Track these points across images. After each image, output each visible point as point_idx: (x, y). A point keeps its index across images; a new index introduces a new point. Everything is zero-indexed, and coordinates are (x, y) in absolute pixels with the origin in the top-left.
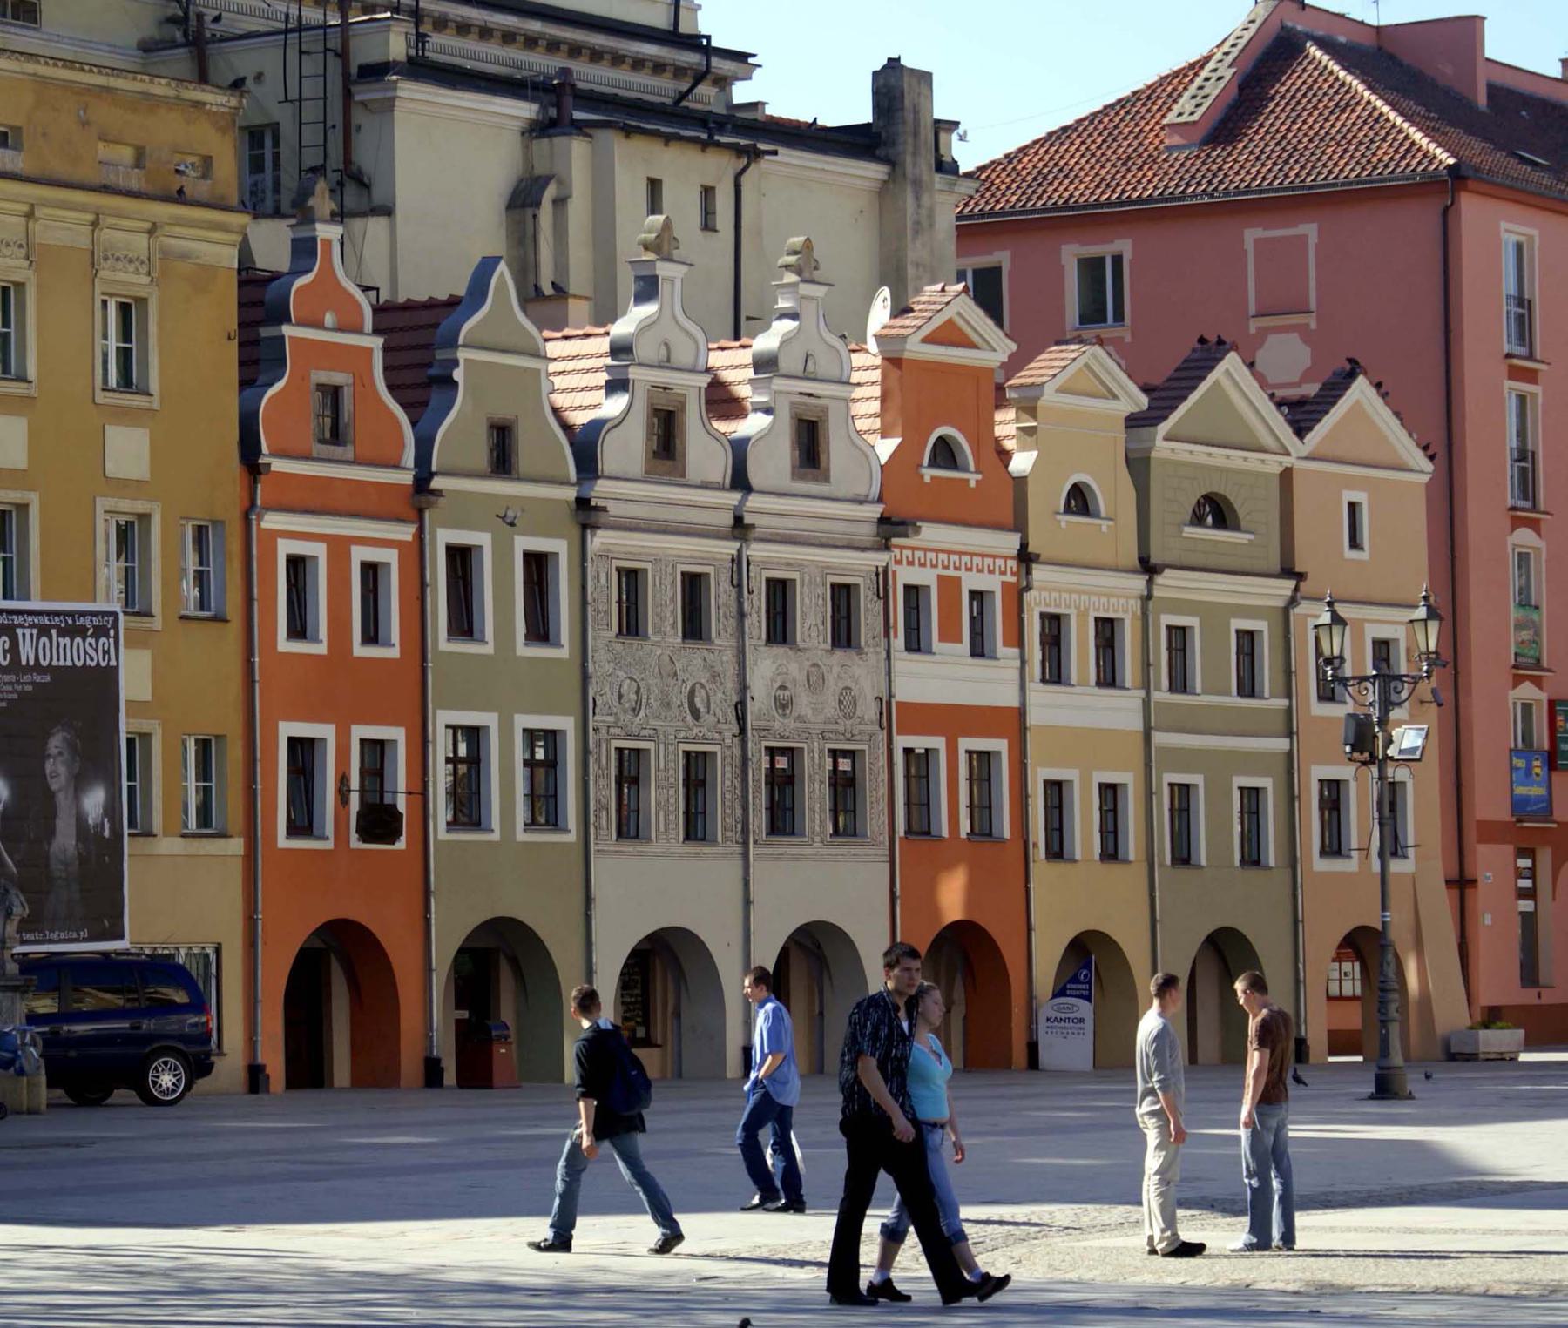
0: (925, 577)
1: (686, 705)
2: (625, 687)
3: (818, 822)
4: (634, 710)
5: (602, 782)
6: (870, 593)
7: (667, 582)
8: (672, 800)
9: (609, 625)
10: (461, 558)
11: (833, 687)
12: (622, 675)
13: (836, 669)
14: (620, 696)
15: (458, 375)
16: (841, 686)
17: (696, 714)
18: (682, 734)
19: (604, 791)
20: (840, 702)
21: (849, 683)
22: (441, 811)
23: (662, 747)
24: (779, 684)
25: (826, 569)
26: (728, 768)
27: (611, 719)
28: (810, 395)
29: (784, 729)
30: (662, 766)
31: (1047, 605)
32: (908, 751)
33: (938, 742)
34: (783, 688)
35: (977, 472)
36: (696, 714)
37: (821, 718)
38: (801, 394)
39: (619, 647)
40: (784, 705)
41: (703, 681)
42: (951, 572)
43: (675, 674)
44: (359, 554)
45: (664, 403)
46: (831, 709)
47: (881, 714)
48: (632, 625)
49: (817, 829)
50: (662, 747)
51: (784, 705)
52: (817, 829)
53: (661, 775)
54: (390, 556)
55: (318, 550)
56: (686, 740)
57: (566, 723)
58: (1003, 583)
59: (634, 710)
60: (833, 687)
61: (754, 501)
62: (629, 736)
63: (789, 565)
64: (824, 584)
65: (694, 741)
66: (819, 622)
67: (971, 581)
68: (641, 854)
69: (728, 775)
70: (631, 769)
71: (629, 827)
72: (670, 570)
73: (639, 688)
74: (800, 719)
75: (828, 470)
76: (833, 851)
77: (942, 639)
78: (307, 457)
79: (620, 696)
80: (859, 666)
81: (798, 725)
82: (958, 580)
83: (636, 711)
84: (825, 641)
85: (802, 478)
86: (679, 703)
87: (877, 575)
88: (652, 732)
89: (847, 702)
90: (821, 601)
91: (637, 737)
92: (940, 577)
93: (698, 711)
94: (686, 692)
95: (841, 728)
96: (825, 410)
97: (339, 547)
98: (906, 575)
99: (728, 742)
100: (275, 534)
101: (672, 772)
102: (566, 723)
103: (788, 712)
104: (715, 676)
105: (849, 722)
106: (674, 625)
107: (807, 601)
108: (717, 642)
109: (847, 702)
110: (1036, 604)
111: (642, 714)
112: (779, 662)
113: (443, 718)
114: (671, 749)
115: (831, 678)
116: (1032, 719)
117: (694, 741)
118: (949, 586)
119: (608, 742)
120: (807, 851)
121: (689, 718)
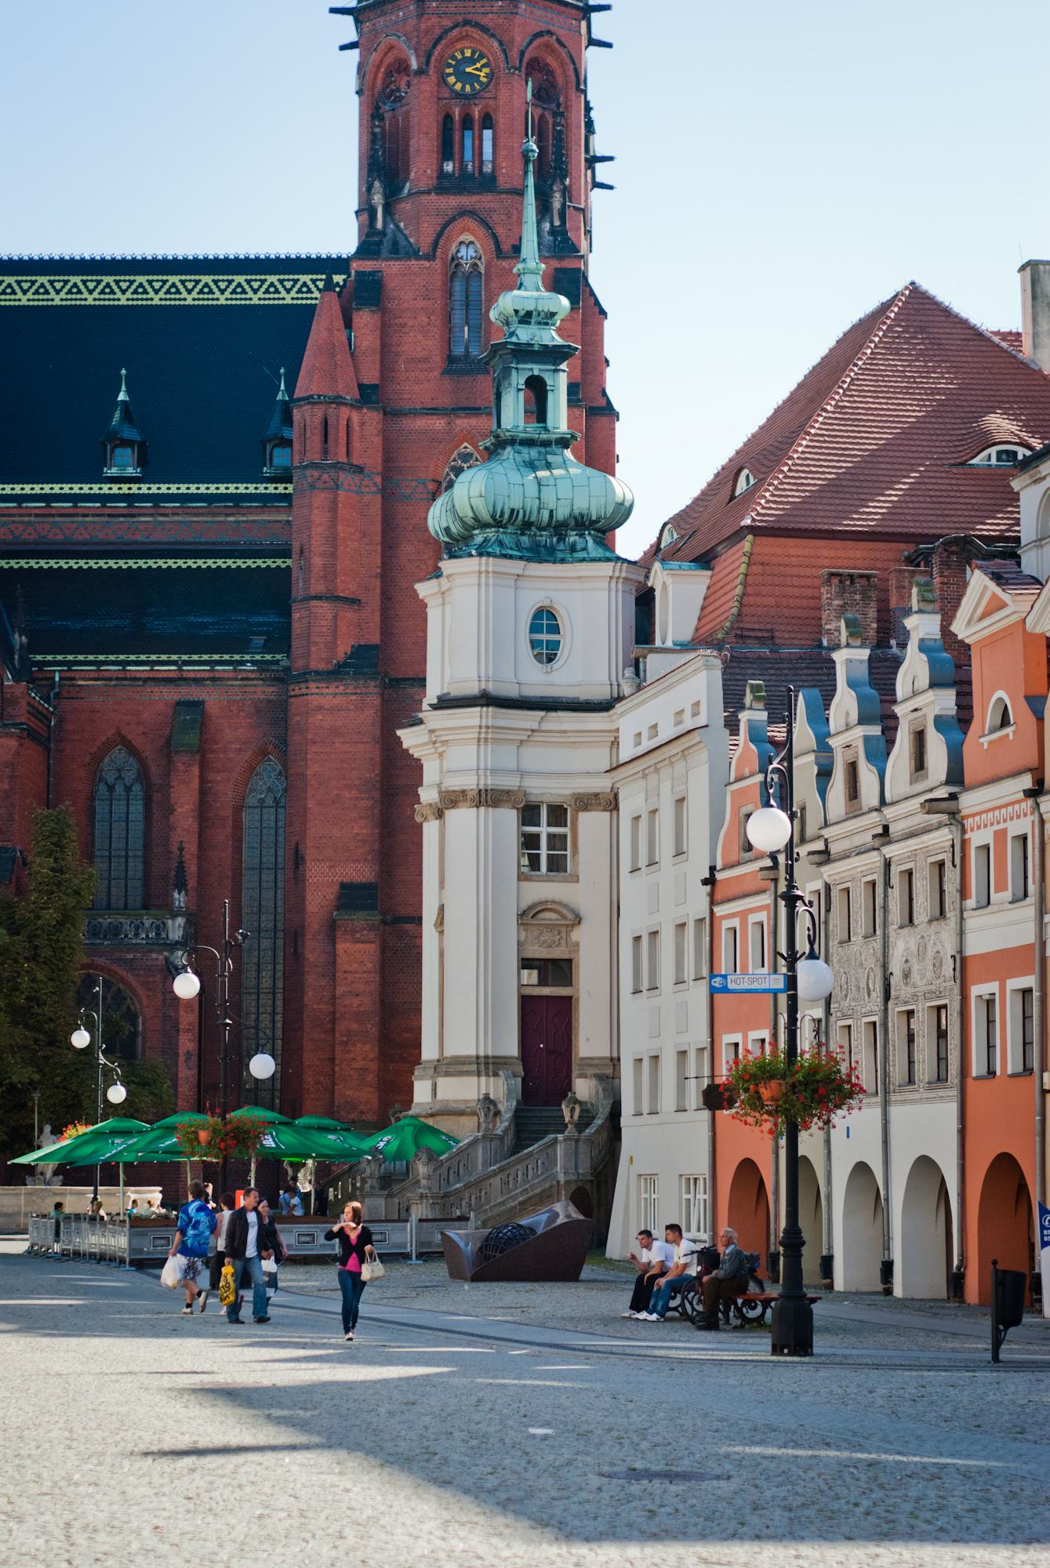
11: (930, 953)
25: (927, 851)
33: (993, 987)
34: (907, 961)
40: (907, 975)
42: (1002, 826)
44: (753, 918)
46: (930, 975)
47: (954, 969)
51: (907, 975)
55: (735, 922)
60: (930, 953)
61: (889, 812)
67: (1016, 828)
78: (738, 864)
82: (1005, 830)
85: (916, 782)
89: (938, 964)
95: (933, 988)
97: (743, 915)
120: (917, 1096)
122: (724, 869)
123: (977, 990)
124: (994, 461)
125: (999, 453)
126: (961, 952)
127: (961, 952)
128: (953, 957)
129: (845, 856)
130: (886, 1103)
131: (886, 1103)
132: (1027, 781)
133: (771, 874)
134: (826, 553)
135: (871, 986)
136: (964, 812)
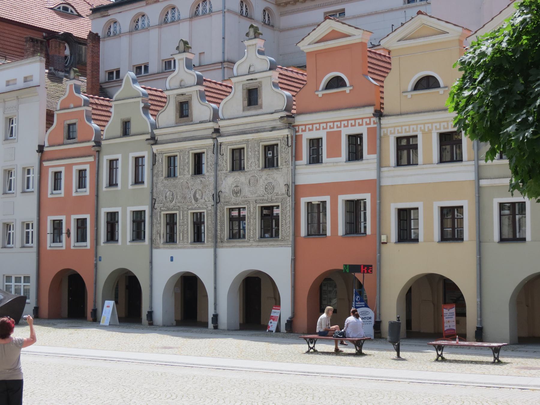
0: (321, 134)
1: (192, 197)
2: (168, 194)
3: (252, 233)
4: (171, 201)
5: (158, 225)
6: (284, 146)
7: (186, 157)
8: (186, 229)
9: (162, 175)
10: (112, 163)
12: (168, 190)
13: (263, 178)
14: (166, 197)
15: (112, 110)
16: (266, 182)
17: (196, 200)
18: (190, 207)
19: (162, 228)
20: (265, 188)
21: (271, 181)
22: (49, 238)
23: (181, 212)
24: (235, 185)
26: (209, 217)
27: (162, 205)
28: (252, 79)
29: (235, 201)
30: (181, 218)
31: (398, 133)
32: (309, 204)
34: (237, 186)
35: (351, 86)
36: (196, 200)
37: (256, 195)
38: (247, 80)
39: (166, 182)
41: (200, 188)
42: (335, 129)
43: (189, 187)
45: (182, 99)
48: (171, 173)
49: (252, 236)
50: (181, 212)
52: (252, 236)
53: (181, 221)
54: (87, 167)
55: (62, 169)
56: (192, 209)
57: (146, 208)
58: (368, 128)
59: (171, 201)
62: (168, 209)
63: (240, 142)
64: (259, 146)
65: (195, 209)
66: (256, 160)
68: (173, 248)
69: (210, 219)
70: (171, 221)
71: (171, 238)
72: (187, 153)
73: (173, 194)
74: (245, 197)
75: (261, 105)
76: (261, 244)
77: (328, 157)
78: (63, 144)
79: (166, 197)
80: (277, 174)
81: (243, 199)
83: (171, 201)
84: (259, 167)
85: (248, 110)
86: (189, 197)
87: (288, 138)
88: (177, 208)
90: (257, 153)
91: (172, 210)
92: (328, 133)
93: (197, 198)
94: (193, 193)
95: (266, 198)
96: (260, 83)
98: (307, 136)
99: (210, 208)
100: (48, 167)
101: (186, 220)
102: (146, 208)
103: (239, 195)
104: (205, 186)
105: (270, 196)
106: (188, 171)
107: (250, 153)
108: (207, 174)
109: (270, 187)
110: (391, 133)
111: (174, 202)
112: (236, 177)
113: (104, 211)
114: (185, 212)
115: (261, 180)
116: (385, 182)
117: (195, 209)
118: (334, 136)
119: (160, 212)
120: (246, 244)
121: (193, 201)
122: (50, 146)
123: (304, 201)
124: (61, 9)
125: (63, 7)
126: (294, 182)
127: (294, 182)
128: (287, 185)
129: (162, 143)
130: (216, 247)
131: (216, 247)
132: (370, 111)
133: (97, 148)
134: (17, 31)
135: (197, 196)
136: (296, 123)
